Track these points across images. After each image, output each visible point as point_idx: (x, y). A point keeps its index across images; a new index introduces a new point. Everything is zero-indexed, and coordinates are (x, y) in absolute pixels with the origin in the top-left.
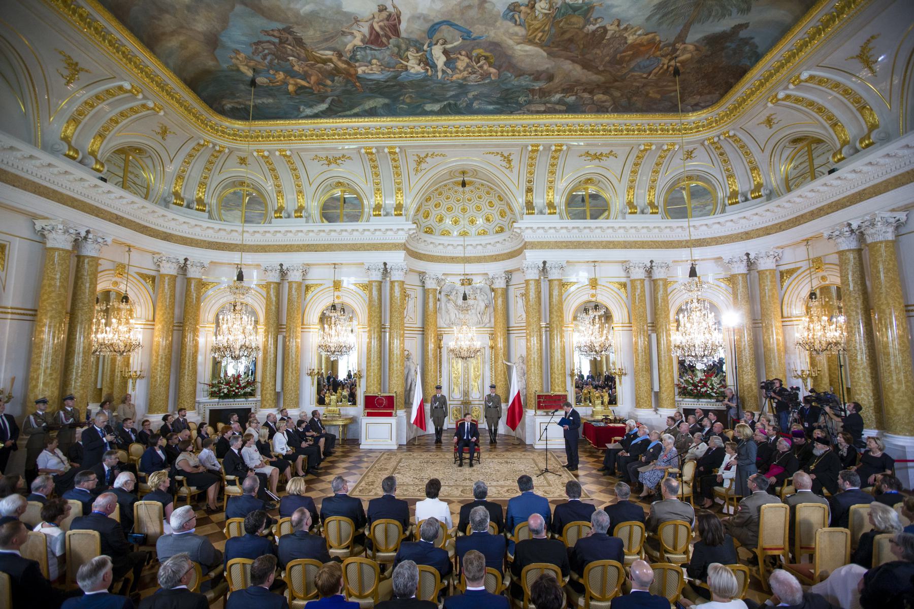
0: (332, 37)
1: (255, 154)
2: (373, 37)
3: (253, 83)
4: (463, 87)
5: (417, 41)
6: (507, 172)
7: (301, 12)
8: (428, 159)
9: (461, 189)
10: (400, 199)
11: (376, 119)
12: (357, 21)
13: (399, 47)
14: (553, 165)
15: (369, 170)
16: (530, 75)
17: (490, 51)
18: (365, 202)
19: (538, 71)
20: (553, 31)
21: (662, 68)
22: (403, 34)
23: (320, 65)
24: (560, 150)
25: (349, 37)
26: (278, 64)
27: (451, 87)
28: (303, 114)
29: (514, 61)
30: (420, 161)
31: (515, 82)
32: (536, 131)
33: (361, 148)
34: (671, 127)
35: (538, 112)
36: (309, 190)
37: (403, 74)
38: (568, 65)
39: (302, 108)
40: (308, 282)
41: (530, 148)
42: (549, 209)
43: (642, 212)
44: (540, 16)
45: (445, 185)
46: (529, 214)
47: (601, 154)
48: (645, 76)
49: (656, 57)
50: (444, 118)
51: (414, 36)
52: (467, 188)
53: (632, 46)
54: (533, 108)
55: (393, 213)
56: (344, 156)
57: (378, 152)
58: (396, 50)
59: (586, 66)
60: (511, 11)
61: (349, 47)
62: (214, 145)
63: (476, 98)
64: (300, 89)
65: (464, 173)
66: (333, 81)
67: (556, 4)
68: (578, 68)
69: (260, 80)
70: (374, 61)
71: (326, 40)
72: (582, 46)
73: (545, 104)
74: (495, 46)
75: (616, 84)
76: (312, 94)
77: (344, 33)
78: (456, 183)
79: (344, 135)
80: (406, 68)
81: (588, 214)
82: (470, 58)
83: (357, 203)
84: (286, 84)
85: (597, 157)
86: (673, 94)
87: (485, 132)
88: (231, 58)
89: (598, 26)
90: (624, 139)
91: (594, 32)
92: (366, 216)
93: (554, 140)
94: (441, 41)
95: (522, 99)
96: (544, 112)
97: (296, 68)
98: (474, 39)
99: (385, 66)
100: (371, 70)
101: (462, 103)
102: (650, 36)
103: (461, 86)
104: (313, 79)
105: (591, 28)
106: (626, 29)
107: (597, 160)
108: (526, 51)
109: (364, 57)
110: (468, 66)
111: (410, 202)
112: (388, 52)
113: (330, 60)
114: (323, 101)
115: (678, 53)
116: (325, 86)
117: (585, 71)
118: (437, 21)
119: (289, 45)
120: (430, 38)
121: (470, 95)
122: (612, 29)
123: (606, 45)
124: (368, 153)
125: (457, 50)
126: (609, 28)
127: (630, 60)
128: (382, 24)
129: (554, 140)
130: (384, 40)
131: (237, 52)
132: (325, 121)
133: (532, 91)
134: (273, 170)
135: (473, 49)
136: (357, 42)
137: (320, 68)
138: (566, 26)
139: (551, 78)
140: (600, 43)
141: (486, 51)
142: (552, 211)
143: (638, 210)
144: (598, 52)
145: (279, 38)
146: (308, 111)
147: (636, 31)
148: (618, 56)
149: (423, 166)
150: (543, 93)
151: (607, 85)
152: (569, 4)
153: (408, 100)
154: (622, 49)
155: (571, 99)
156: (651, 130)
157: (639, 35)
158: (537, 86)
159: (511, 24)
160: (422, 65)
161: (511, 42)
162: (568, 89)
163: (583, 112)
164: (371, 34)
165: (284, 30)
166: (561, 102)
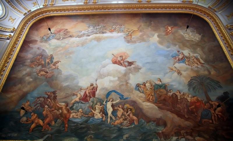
0: (68, 96)
12: (81, 89)
13: (93, 102)
16: (154, 121)
17: (133, 106)
19: (157, 119)
20: (156, 95)
22: (97, 96)
23: (56, 111)
25: (75, 96)
27: (114, 130)
29: (144, 111)
37: (91, 120)
38: (170, 115)
44: (149, 89)
51: (101, 97)
58: (91, 104)
59: (179, 115)
61: (73, 101)
68: (175, 116)
70: (80, 110)
71: (66, 97)
72: (171, 103)
74: (134, 103)
75: (201, 128)
77: (74, 95)
82: (124, 110)
89: (172, 93)
91: (172, 95)
94: (111, 100)
97: (44, 113)
98: (125, 99)
100: (77, 115)
105: (170, 94)
106: (184, 94)
108: (148, 106)
109: (77, 107)
110: (123, 114)
112: (88, 105)
113: (61, 108)
115: (214, 106)
118: (110, 90)
119: (50, 99)
120: (107, 98)
121: (125, 137)
125: (118, 104)
126: (177, 94)
128: (90, 91)
130: (88, 98)
135: (125, 104)
137: (54, 113)
144: (180, 106)
145: (49, 96)
147: (188, 95)
152: (157, 84)
158: (161, 129)
159: (138, 92)
160: (101, 113)
161: (140, 101)
164: (84, 95)
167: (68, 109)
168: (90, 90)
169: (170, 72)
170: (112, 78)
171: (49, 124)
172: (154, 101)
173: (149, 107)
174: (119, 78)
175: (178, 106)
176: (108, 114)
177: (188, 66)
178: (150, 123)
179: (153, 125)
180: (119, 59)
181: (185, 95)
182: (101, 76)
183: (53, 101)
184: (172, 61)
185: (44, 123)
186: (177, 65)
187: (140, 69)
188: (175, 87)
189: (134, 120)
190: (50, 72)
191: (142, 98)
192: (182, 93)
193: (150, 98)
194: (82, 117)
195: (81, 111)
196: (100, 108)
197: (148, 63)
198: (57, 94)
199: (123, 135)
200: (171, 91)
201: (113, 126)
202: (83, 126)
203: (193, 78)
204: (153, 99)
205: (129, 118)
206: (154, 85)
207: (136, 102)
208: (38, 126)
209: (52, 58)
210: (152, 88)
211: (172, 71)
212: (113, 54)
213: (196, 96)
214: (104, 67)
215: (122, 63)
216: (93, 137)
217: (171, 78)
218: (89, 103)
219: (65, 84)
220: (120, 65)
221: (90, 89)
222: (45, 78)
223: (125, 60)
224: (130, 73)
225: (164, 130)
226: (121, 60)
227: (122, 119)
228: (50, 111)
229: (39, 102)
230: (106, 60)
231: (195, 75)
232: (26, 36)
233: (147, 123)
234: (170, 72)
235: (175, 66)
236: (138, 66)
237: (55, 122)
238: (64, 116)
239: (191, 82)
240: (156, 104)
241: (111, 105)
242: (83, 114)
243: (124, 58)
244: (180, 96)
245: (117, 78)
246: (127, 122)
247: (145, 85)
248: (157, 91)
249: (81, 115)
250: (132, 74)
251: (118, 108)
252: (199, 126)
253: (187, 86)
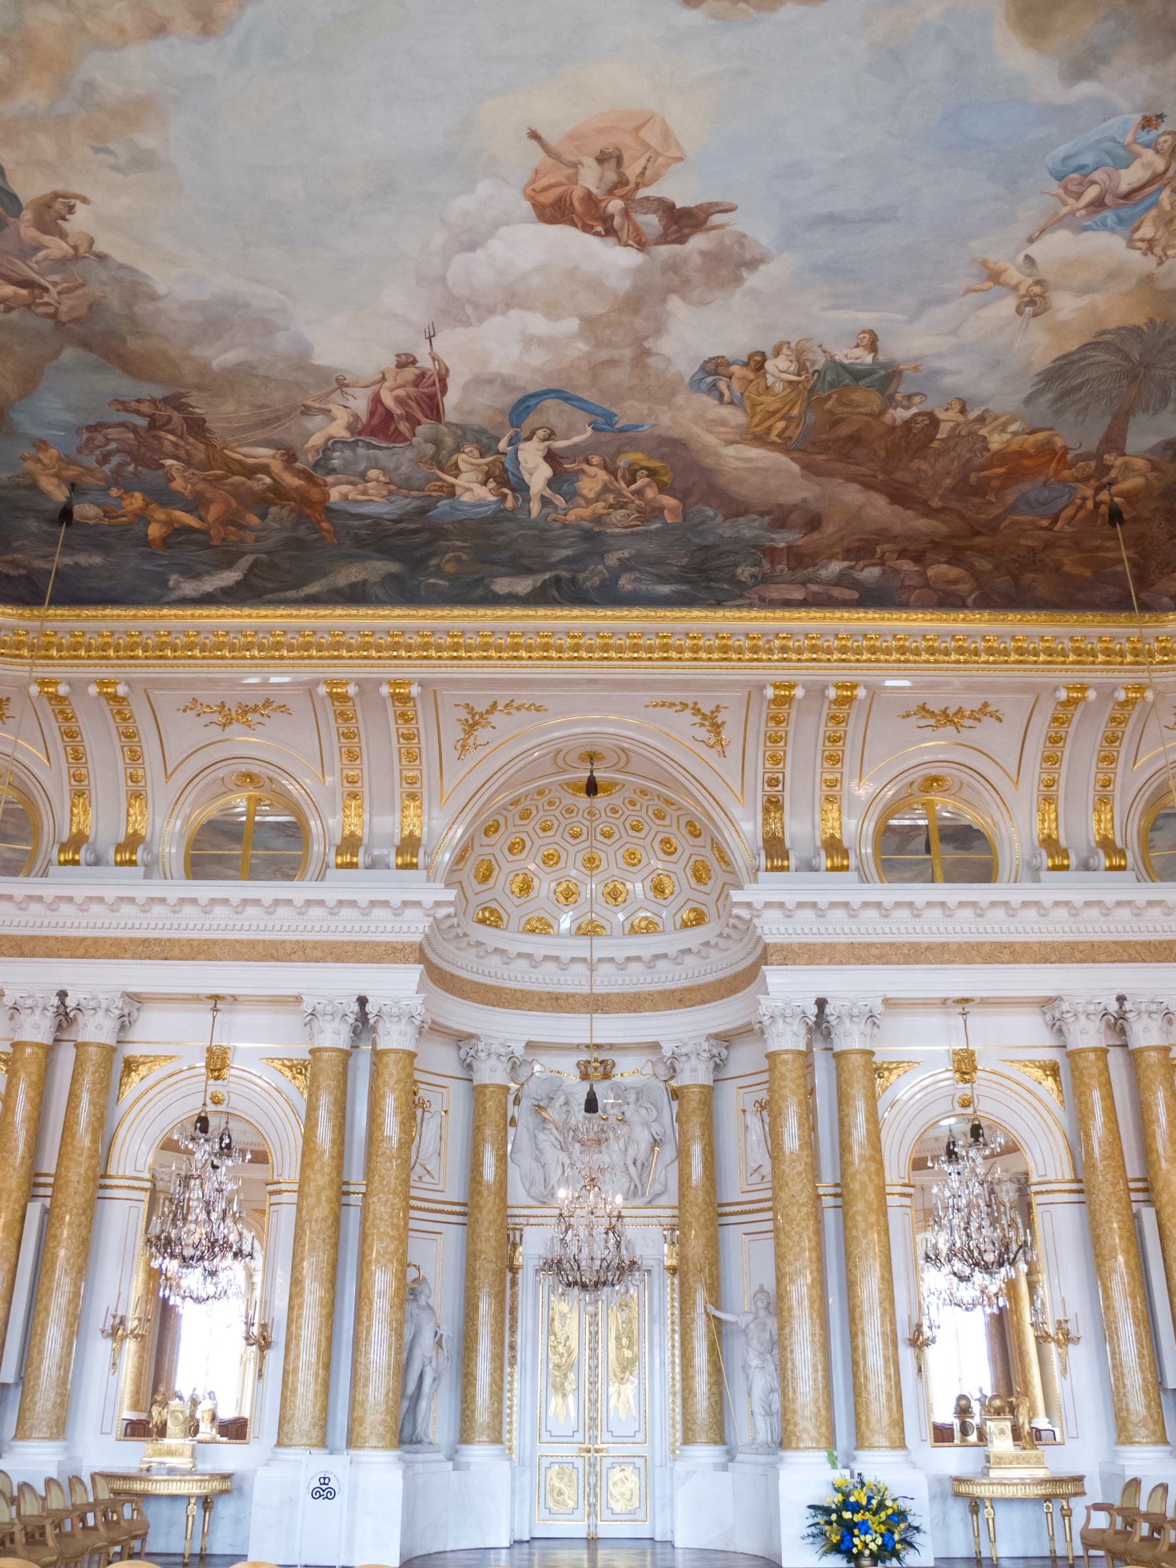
0: (278, 419)
1: (34, 689)
2: (376, 421)
3: (66, 515)
4: (593, 539)
5: (481, 432)
6: (710, 755)
7: (216, 364)
8: (496, 718)
9: (583, 801)
10: (414, 823)
11: (363, 611)
12: (342, 384)
14: (834, 740)
15: (333, 744)
16: (762, 514)
17: (663, 458)
18: (314, 825)
19: (780, 506)
20: (811, 418)
21: (1081, 507)
22: (450, 415)
24: (849, 700)
25: (319, 419)
26: (136, 474)
28: (178, 594)
30: (473, 722)
31: (726, 530)
32: (784, 649)
33: (317, 683)
34: (1127, 646)
35: (787, 604)
36: (160, 791)
37: (443, 505)
38: (853, 495)
39: (173, 579)
40: (130, 1051)
41: (770, 693)
42: (829, 856)
43: (1086, 867)
44: (778, 387)
45: (540, 792)
46: (775, 869)
47: (960, 711)
48: (1045, 523)
49: (1064, 482)
50: (541, 612)
51: (475, 421)
52: (600, 801)
53: (1002, 457)
54: (774, 593)
55: (393, 860)
56: (267, 703)
57: (362, 692)
58: (430, 449)
59: (899, 496)
60: (710, 374)
61: (317, 440)
63: (625, 566)
64: (177, 534)
65: (592, 757)
66: (263, 516)
67: (813, 363)
69: (85, 510)
70: (373, 473)
71: (264, 424)
72: (882, 454)
73: (804, 584)
75: (979, 540)
76: (207, 546)
77: (307, 411)
78: (572, 786)
79: (273, 649)
80: (451, 491)
81: (938, 872)
83: (296, 832)
84: (143, 518)
85: (948, 718)
86: (1119, 568)
87: (650, 649)
88: (24, 459)
89: (914, 410)
90: (1016, 675)
92: (313, 866)
93: (832, 674)
95: (744, 572)
96: (804, 604)
97: (178, 485)
98: (622, 430)
99: (398, 485)
100: (364, 493)
101: (591, 577)
102: (1041, 436)
103: (588, 536)
104: (214, 512)
105: (901, 415)
106: (981, 419)
107: (950, 729)
108: (749, 460)
109: (347, 464)
110: (606, 489)
111: (444, 829)
112: (410, 454)
113: (265, 469)
114: (229, 564)
116: (242, 527)
117: (898, 509)
118: (532, 389)
119: (172, 432)
121: (612, 559)
122: (948, 419)
123: (939, 453)
124: (334, 697)
125: (581, 453)
126: (941, 415)
127: (1003, 487)
128: (401, 392)
129: (832, 674)
130: (403, 427)
131: (41, 445)
132: (231, 611)
133: (771, 553)
134: (70, 734)
135: (619, 452)
136: (338, 429)
138: (840, 410)
139: (814, 523)
140: (925, 446)
141: (650, 456)
142: (838, 861)
143: (1073, 861)
144: (924, 466)
145: (152, 417)
146: (189, 588)
147: (1005, 425)
148: (973, 477)
149: (482, 734)
150: (799, 559)
151: (956, 543)
152: (842, 366)
153: (450, 568)
154: (978, 461)
155: (870, 574)
156: (1078, 651)
157: (1015, 434)
158: (782, 539)
159: (710, 401)
160: (492, 484)
161: (711, 439)
162: (861, 551)
163: (904, 605)
164: (372, 414)
165: (165, 400)
166: (841, 580)
167: (304, 471)
168: (403, 386)
169: (969, 291)
170: (538, 324)
172: (789, 443)
173: (754, 464)
174: (589, 323)
175: (918, 464)
176: (527, 488)
177: (1137, 254)
178: (741, 520)
179: (757, 524)
180: (591, 178)
181: (988, 421)
182: (461, 308)
183: (191, 440)
184: (1042, 195)
186: (1057, 246)
187: (753, 264)
188: (949, 381)
189: (661, 509)
190: (55, 284)
191: (723, 429)
192: (979, 413)
193: (770, 428)
194: (393, 498)
195: (382, 478)
196: (479, 465)
197: (832, 219)
198: (198, 411)
199: (607, 552)
200: (917, 399)
201: (557, 525)
202: (413, 526)
203: (1107, 337)
204: (788, 433)
205: (637, 502)
206: (818, 367)
207: (684, 445)
210: (799, 382)
211: (990, 284)
212: (534, 135)
213: (1050, 429)
214: (472, 246)
215: (612, 216)
216: (464, 557)
217: (954, 332)
218: (411, 445)
219: (223, 356)
220: (600, 229)
221: (400, 381)
222: (51, 322)
223: (643, 193)
224: (673, 291)
225: (799, 543)
226: (611, 192)
227: (601, 504)
228: (205, 480)
230: (484, 188)
231: (1139, 320)
233: (726, 518)
234: (969, 291)
235: (1034, 250)
236: (742, 245)
238: (298, 498)
239: (1075, 358)
240: (797, 455)
241: (541, 454)
242: (392, 487)
243: (632, 171)
244: (958, 424)
245: (572, 324)
246: (629, 516)
247: (760, 368)
248: (829, 397)
249: (385, 493)
250: (683, 298)
251: (585, 467)
252: (976, 533)
253: (1037, 379)
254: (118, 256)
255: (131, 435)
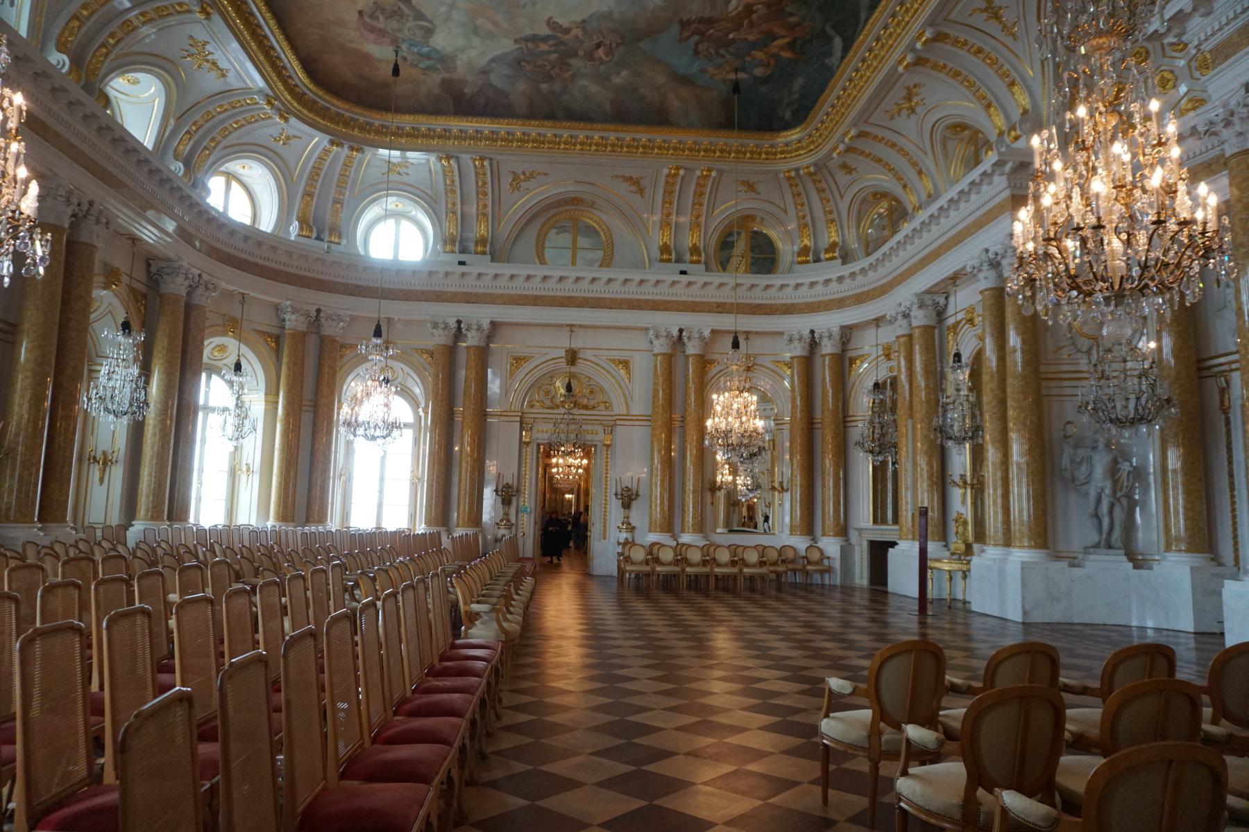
23: (754, 17)
62: (797, 170)
114: (829, 40)
116: (798, 24)
131: (703, 71)
146: (834, 60)
171: (793, 27)
185: (783, 37)
208: (791, 46)
209: (534, 39)
229: (712, 51)
232: (437, 112)
237: (791, 14)
254: (585, 16)
255: (706, 44)
